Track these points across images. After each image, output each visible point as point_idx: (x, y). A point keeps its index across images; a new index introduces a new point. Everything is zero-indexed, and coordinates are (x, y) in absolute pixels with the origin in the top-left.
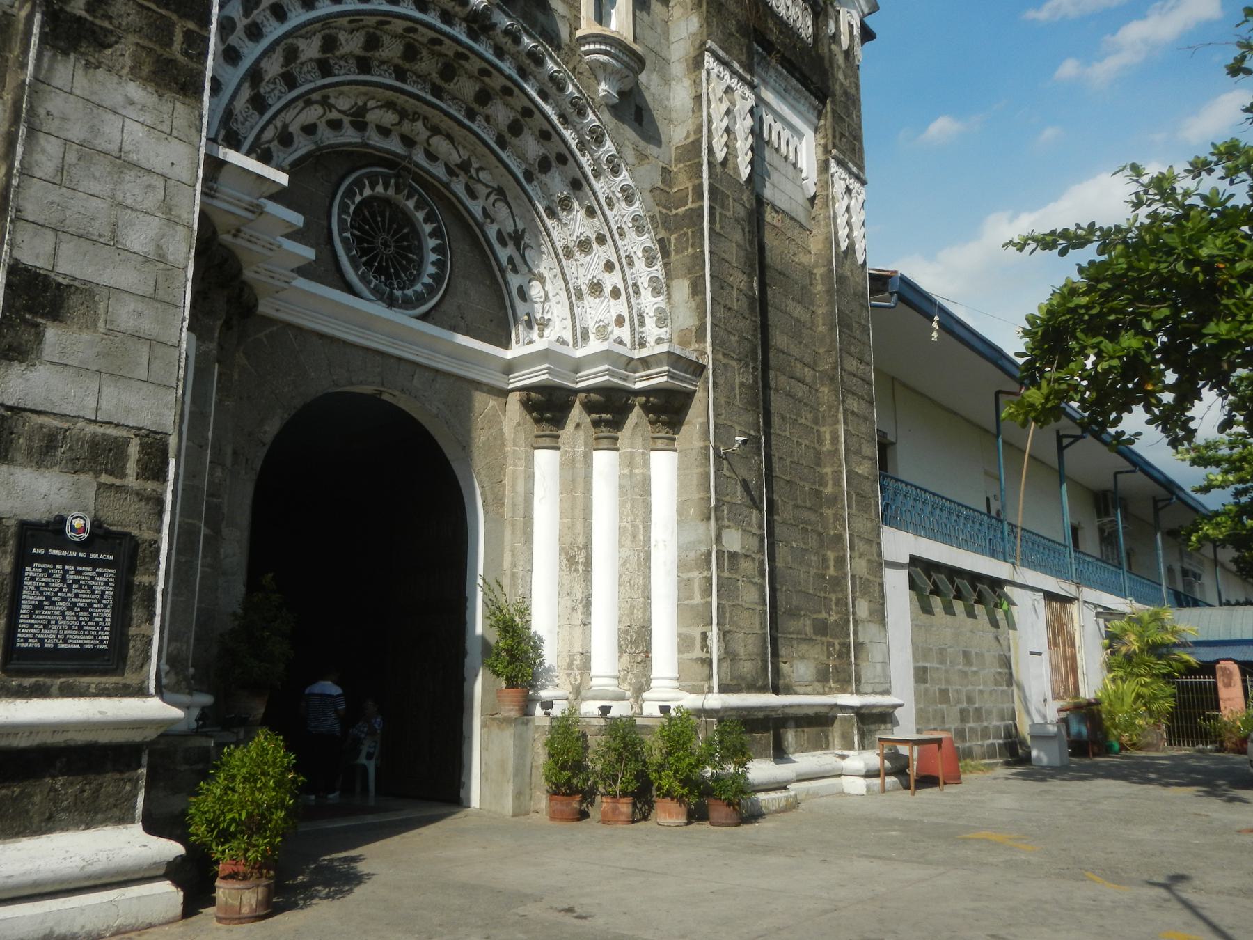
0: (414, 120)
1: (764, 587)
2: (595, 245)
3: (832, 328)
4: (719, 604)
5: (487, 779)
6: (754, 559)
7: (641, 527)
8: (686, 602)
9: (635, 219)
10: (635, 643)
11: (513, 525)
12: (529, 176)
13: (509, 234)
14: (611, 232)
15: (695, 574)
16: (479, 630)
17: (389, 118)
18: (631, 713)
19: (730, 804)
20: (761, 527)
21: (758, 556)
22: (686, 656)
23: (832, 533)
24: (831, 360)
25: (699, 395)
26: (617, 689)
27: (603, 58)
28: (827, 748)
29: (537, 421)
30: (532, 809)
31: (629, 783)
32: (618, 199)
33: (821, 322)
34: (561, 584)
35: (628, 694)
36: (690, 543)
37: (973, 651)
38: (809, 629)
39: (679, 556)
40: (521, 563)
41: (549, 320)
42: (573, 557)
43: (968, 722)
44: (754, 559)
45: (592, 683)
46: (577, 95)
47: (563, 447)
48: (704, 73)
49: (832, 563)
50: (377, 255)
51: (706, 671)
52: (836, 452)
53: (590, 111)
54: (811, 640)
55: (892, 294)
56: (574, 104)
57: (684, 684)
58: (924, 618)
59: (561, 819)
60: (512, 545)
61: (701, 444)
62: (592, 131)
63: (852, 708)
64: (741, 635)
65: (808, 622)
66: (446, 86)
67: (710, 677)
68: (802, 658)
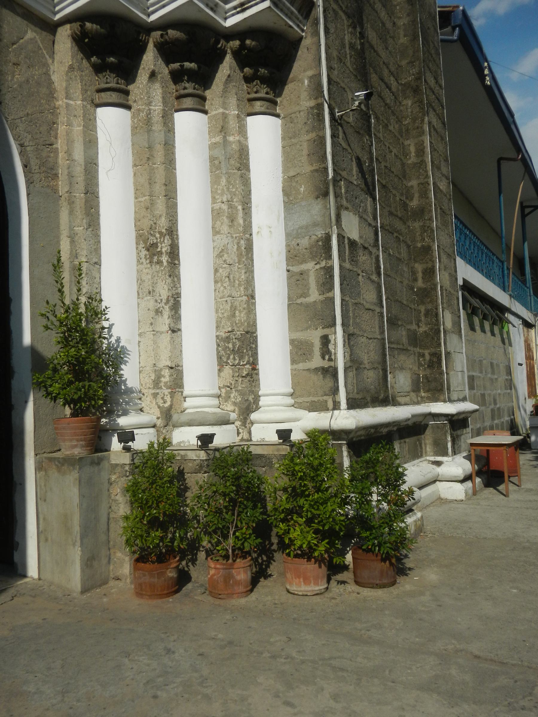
1: (380, 287)
3: (415, 38)
4: (342, 300)
5: (47, 540)
6: (370, 253)
7: (240, 208)
8: (299, 301)
10: (238, 352)
11: (71, 203)
15: (310, 266)
16: (27, 339)
18: (237, 440)
19: (386, 558)
20: (375, 218)
21: (374, 251)
22: (301, 366)
23: (419, 245)
24: (414, 71)
25: (307, 42)
26: (218, 410)
28: (421, 456)
29: (98, 69)
30: (112, 576)
31: (246, 539)
33: (402, 33)
34: (140, 281)
35: (233, 416)
36: (301, 228)
37: (495, 362)
38: (405, 340)
39: (287, 245)
40: (85, 252)
42: (154, 245)
43: (495, 420)
44: (370, 253)
45: (186, 405)
47: (135, 106)
49: (420, 275)
51: (329, 383)
52: (423, 163)
54: (407, 350)
55: (454, 28)
57: (300, 400)
58: (471, 332)
59: (152, 596)
60: (71, 229)
61: (312, 103)
63: (446, 416)
64: (364, 340)
65: (404, 333)
67: (335, 391)
68: (402, 369)
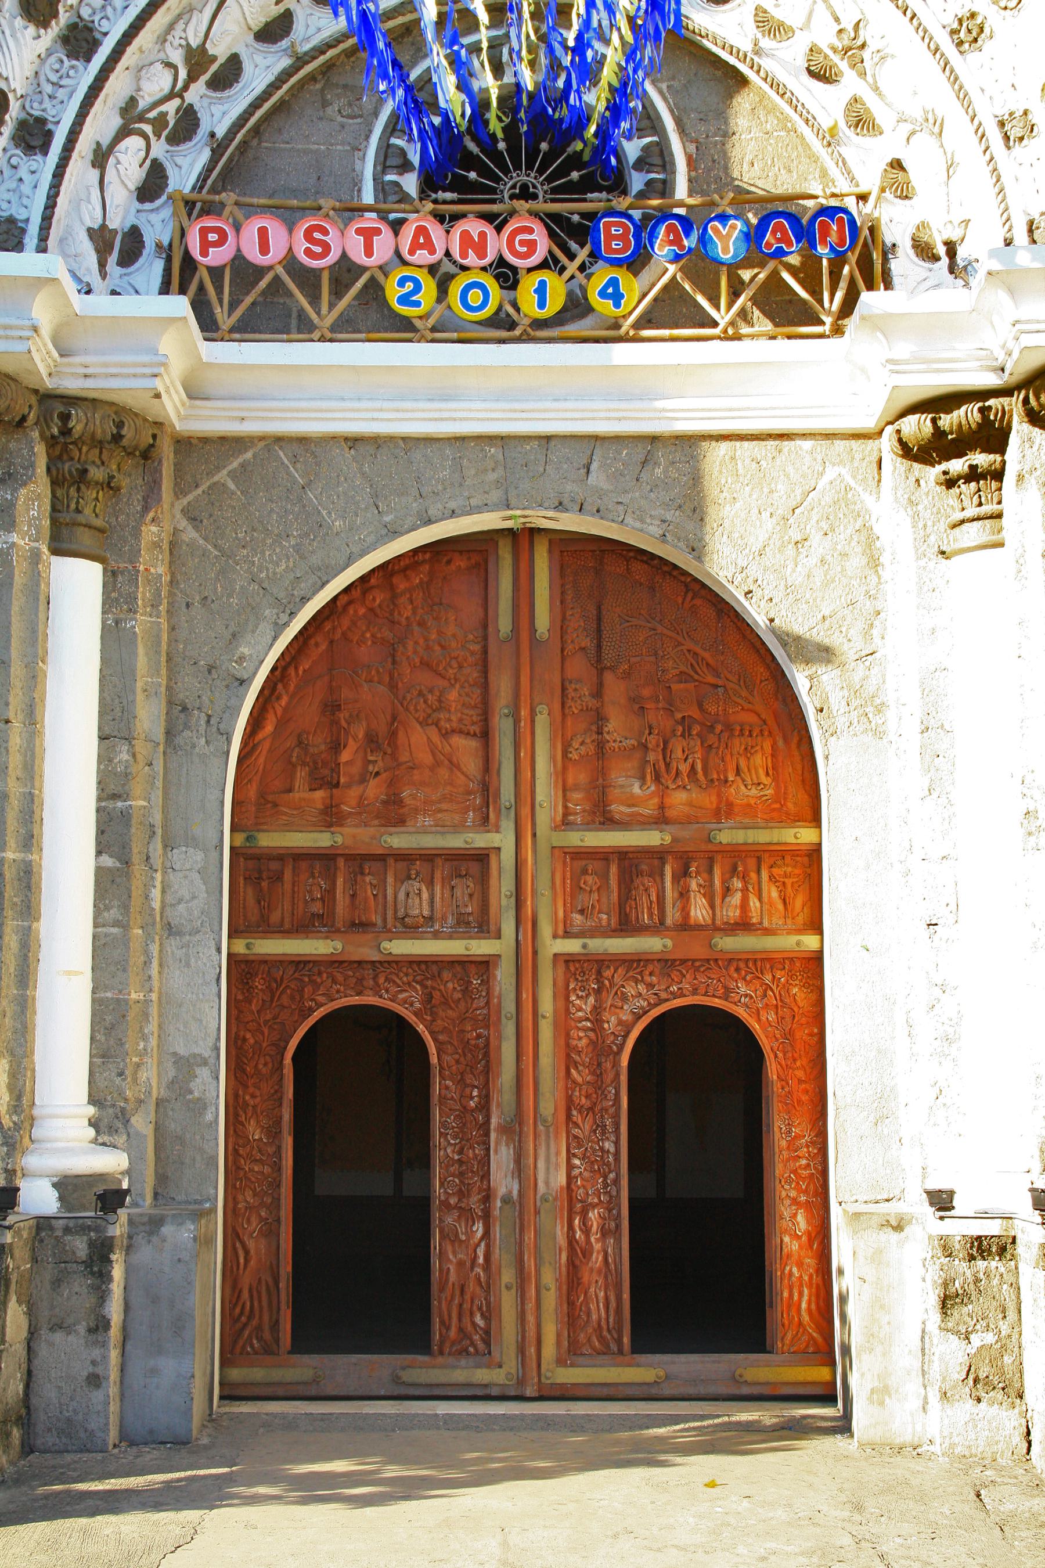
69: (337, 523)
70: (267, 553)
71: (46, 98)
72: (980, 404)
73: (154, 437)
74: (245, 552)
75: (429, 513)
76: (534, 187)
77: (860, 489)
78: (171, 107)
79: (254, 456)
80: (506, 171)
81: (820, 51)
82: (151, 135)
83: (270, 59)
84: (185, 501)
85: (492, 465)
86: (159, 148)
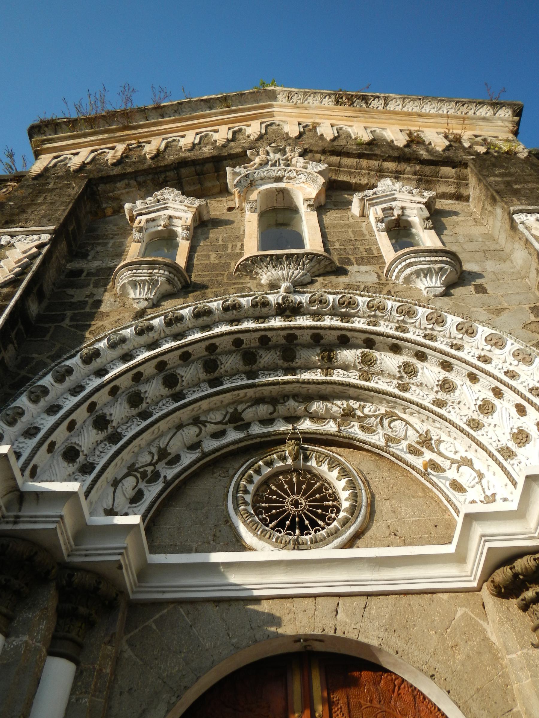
0: (285, 402)
2: (496, 402)
9: (516, 354)
12: (404, 388)
13: (418, 443)
14: (501, 381)
17: (263, 410)
27: (409, 270)
32: (490, 351)
41: (494, 495)
46: (400, 304)
48: (521, 227)
50: (289, 514)
53: (417, 307)
56: (399, 311)
62: (429, 319)
66: (294, 365)
69: (207, 645)
70: (169, 662)
71: (96, 456)
72: (533, 557)
73: (117, 595)
74: (157, 662)
75: (257, 637)
76: (301, 507)
77: (477, 619)
78: (150, 469)
79: (168, 611)
80: (289, 496)
81: (412, 446)
82: (139, 478)
83: (192, 455)
84: (129, 636)
85: (288, 611)
86: (142, 485)
